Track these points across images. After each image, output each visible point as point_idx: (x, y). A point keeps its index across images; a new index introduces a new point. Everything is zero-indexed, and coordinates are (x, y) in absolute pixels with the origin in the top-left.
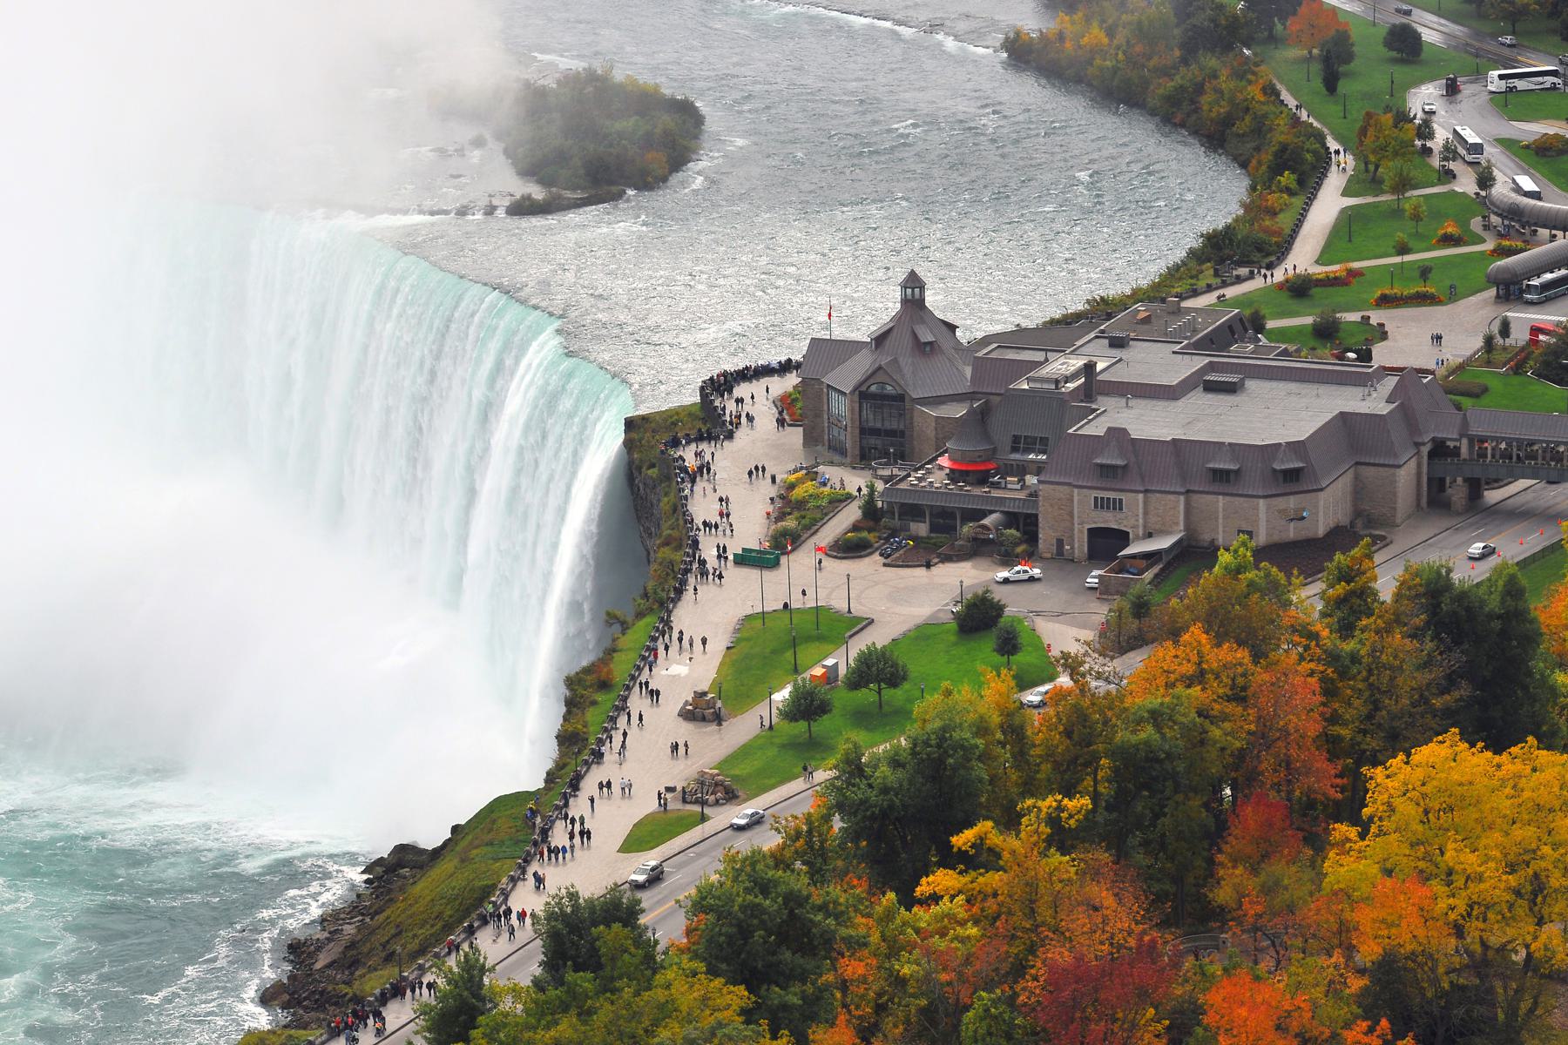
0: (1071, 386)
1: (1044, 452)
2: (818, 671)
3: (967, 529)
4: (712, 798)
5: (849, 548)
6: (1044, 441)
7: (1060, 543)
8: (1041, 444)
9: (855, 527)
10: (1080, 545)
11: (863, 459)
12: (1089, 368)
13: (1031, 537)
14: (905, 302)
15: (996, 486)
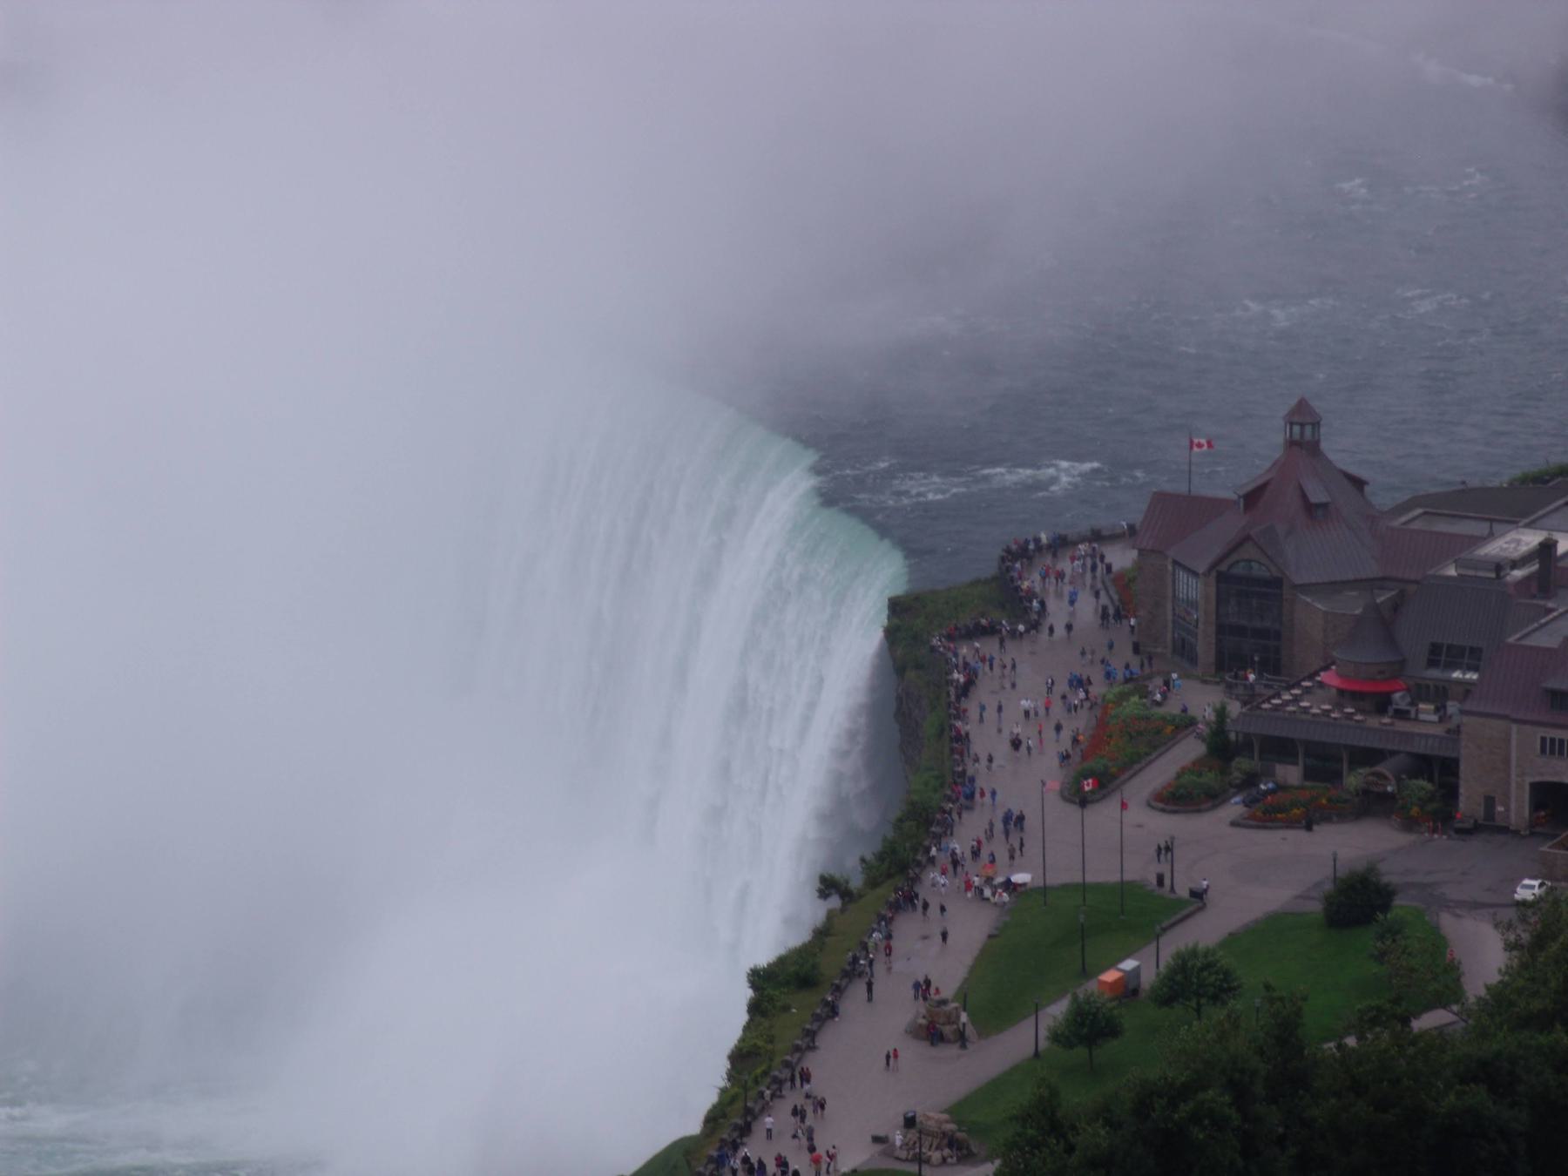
0: (1518, 574)
1: (1476, 669)
2: (1110, 976)
3: (1353, 780)
4: (936, 1156)
5: (1176, 799)
6: (1476, 652)
7: (1490, 802)
8: (1470, 657)
9: (1197, 766)
10: (1517, 808)
11: (1228, 664)
12: (1547, 548)
13: (1450, 792)
14: (1291, 444)
15: (1401, 715)
